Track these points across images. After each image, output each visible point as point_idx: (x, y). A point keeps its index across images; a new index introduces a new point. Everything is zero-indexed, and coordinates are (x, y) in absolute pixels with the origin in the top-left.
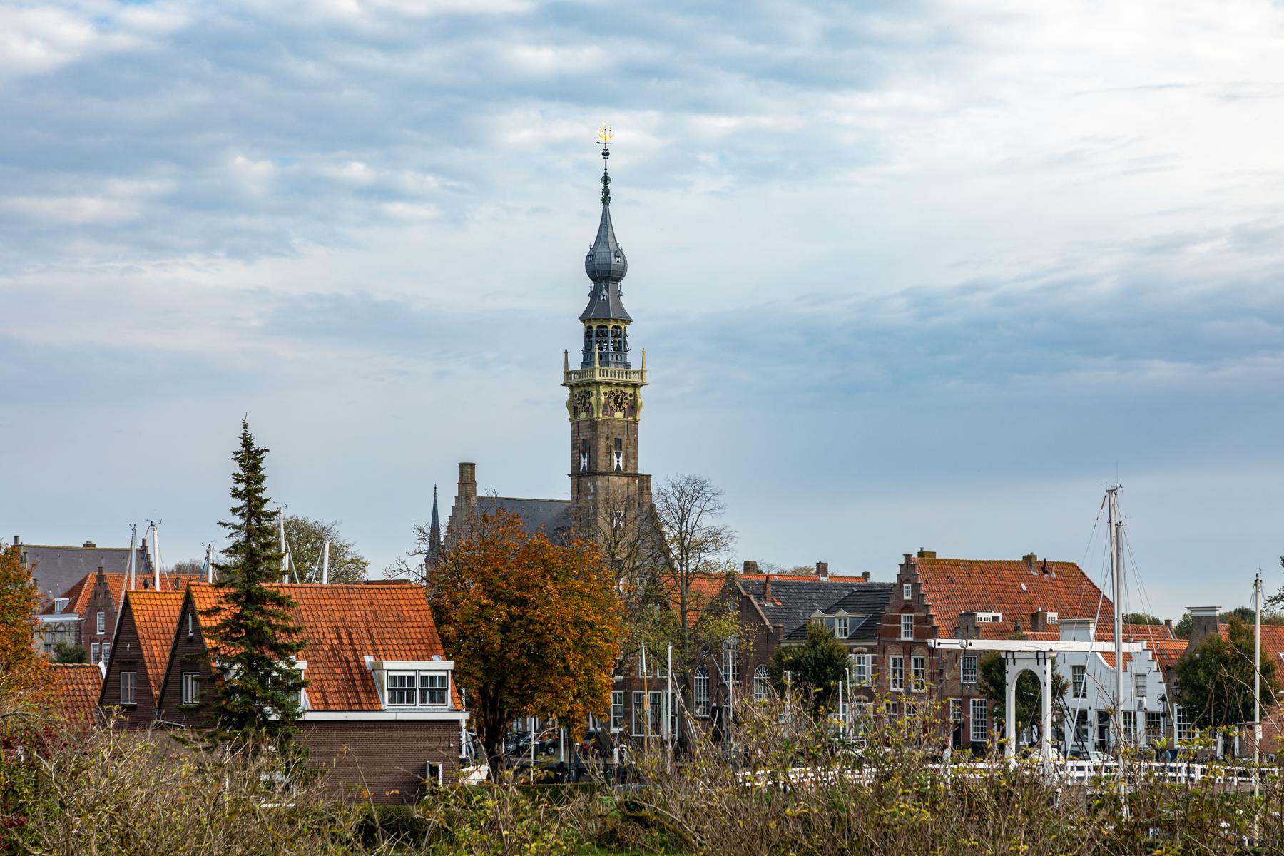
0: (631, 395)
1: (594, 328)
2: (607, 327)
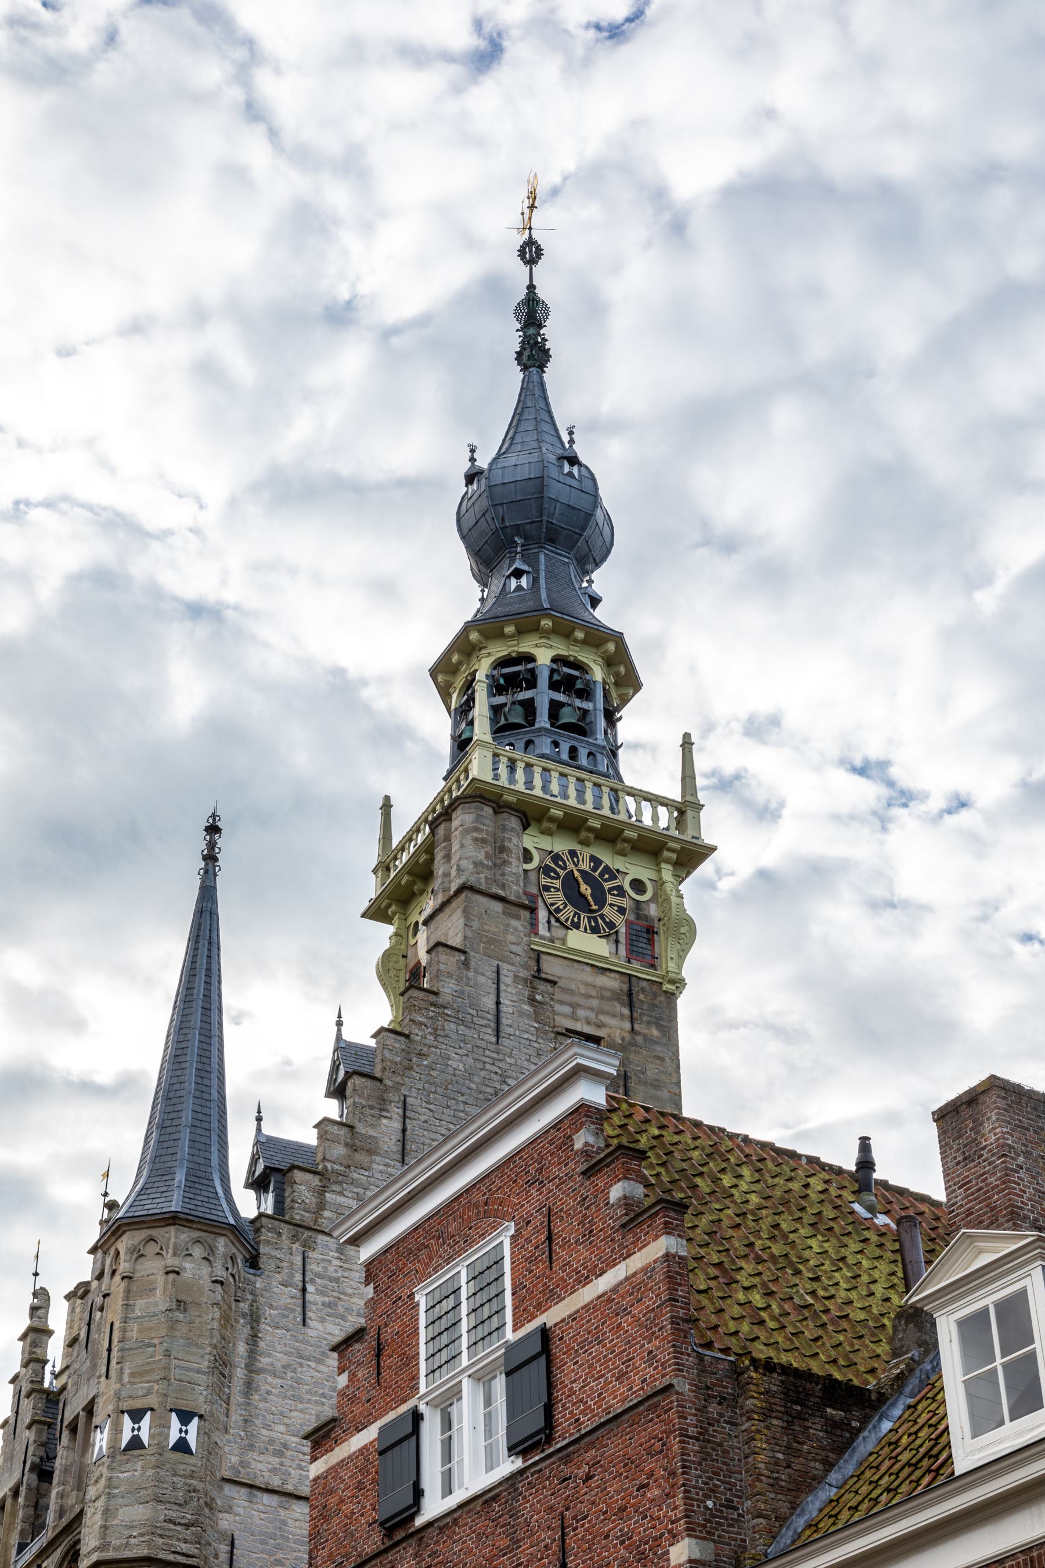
0: (638, 885)
2: (531, 658)
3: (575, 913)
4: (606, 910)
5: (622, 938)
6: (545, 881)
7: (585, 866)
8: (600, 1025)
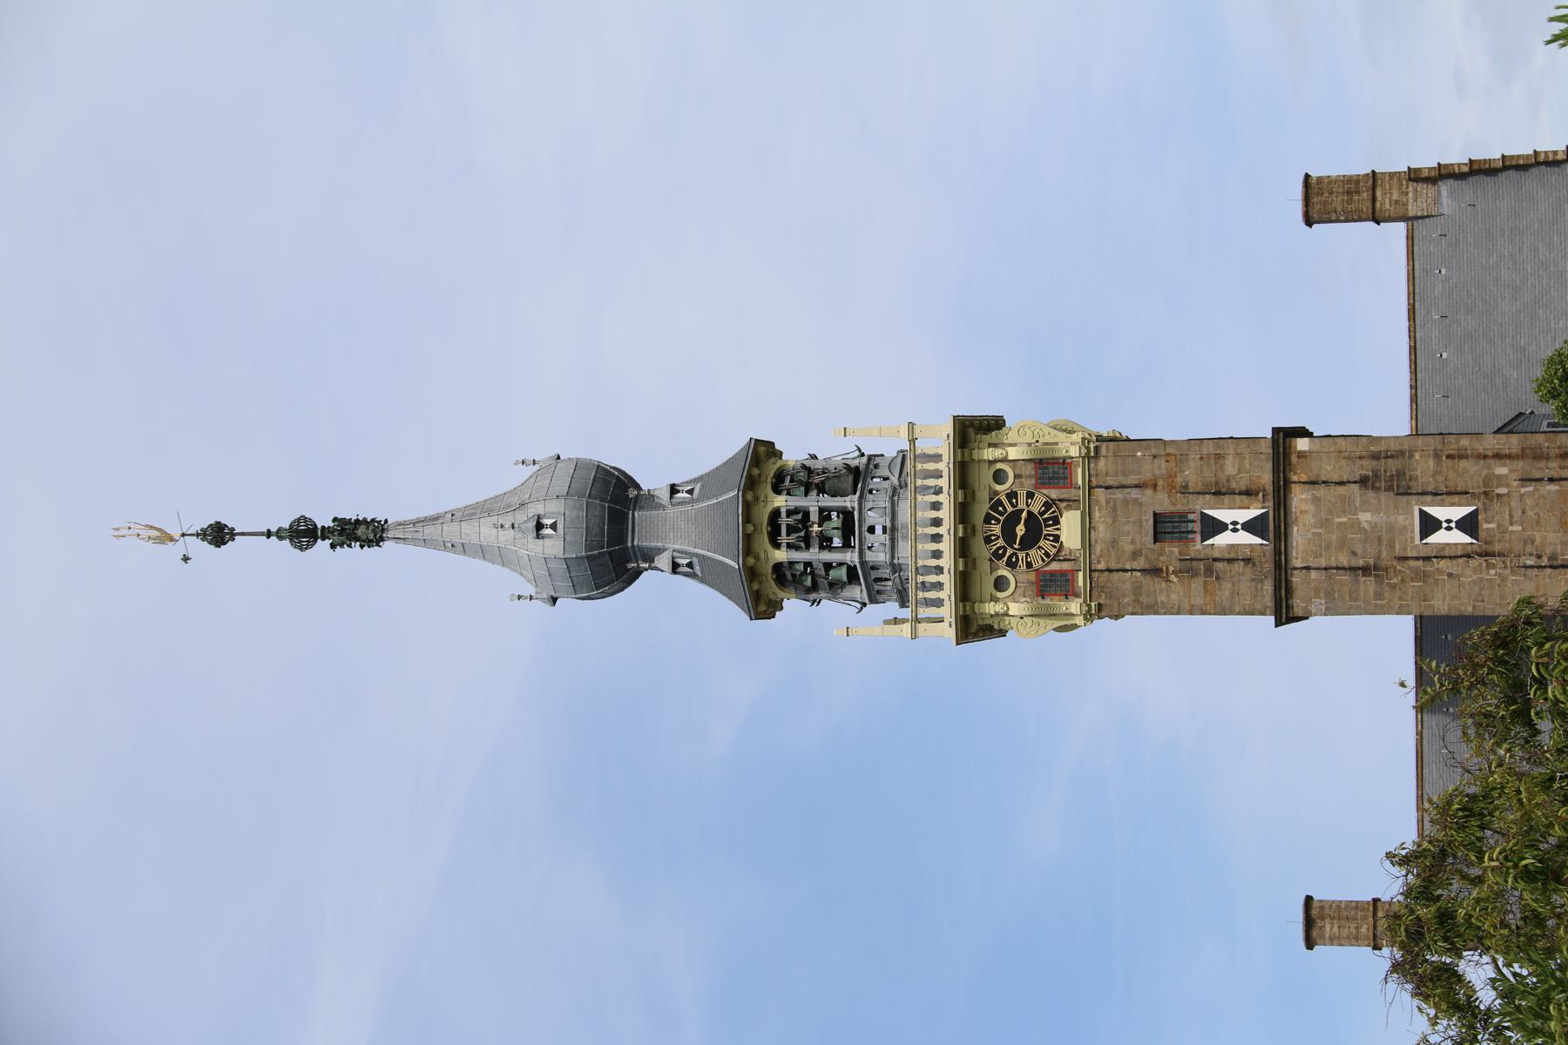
3: (1045, 538)
5: (1054, 494)
6: (1022, 566)
7: (997, 529)
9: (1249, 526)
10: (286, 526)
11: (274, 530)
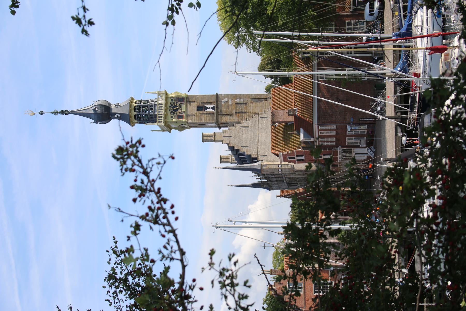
0: (172, 100)
1: (137, 121)
2: (135, 116)
4: (177, 105)
7: (171, 108)
8: (195, 106)
9: (212, 108)
10: (53, 111)
11: (51, 112)
